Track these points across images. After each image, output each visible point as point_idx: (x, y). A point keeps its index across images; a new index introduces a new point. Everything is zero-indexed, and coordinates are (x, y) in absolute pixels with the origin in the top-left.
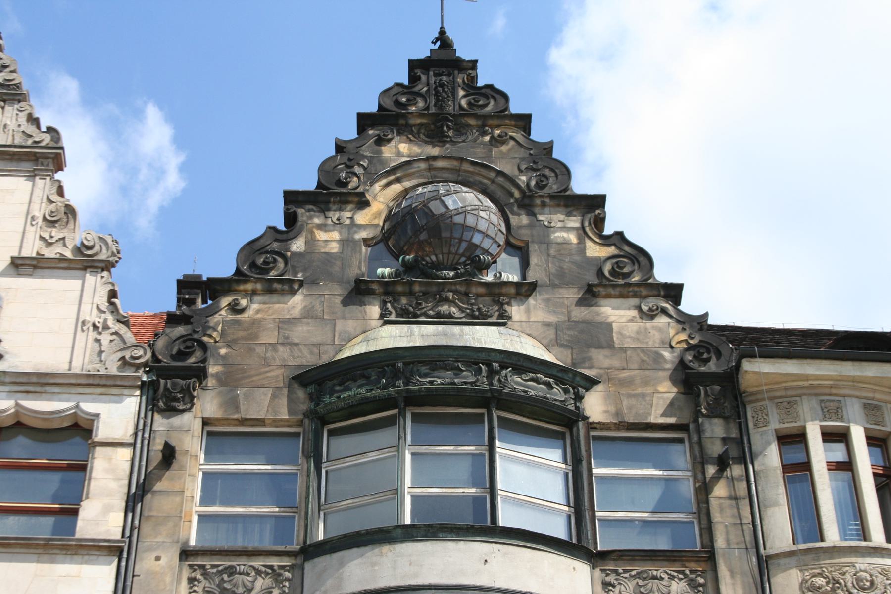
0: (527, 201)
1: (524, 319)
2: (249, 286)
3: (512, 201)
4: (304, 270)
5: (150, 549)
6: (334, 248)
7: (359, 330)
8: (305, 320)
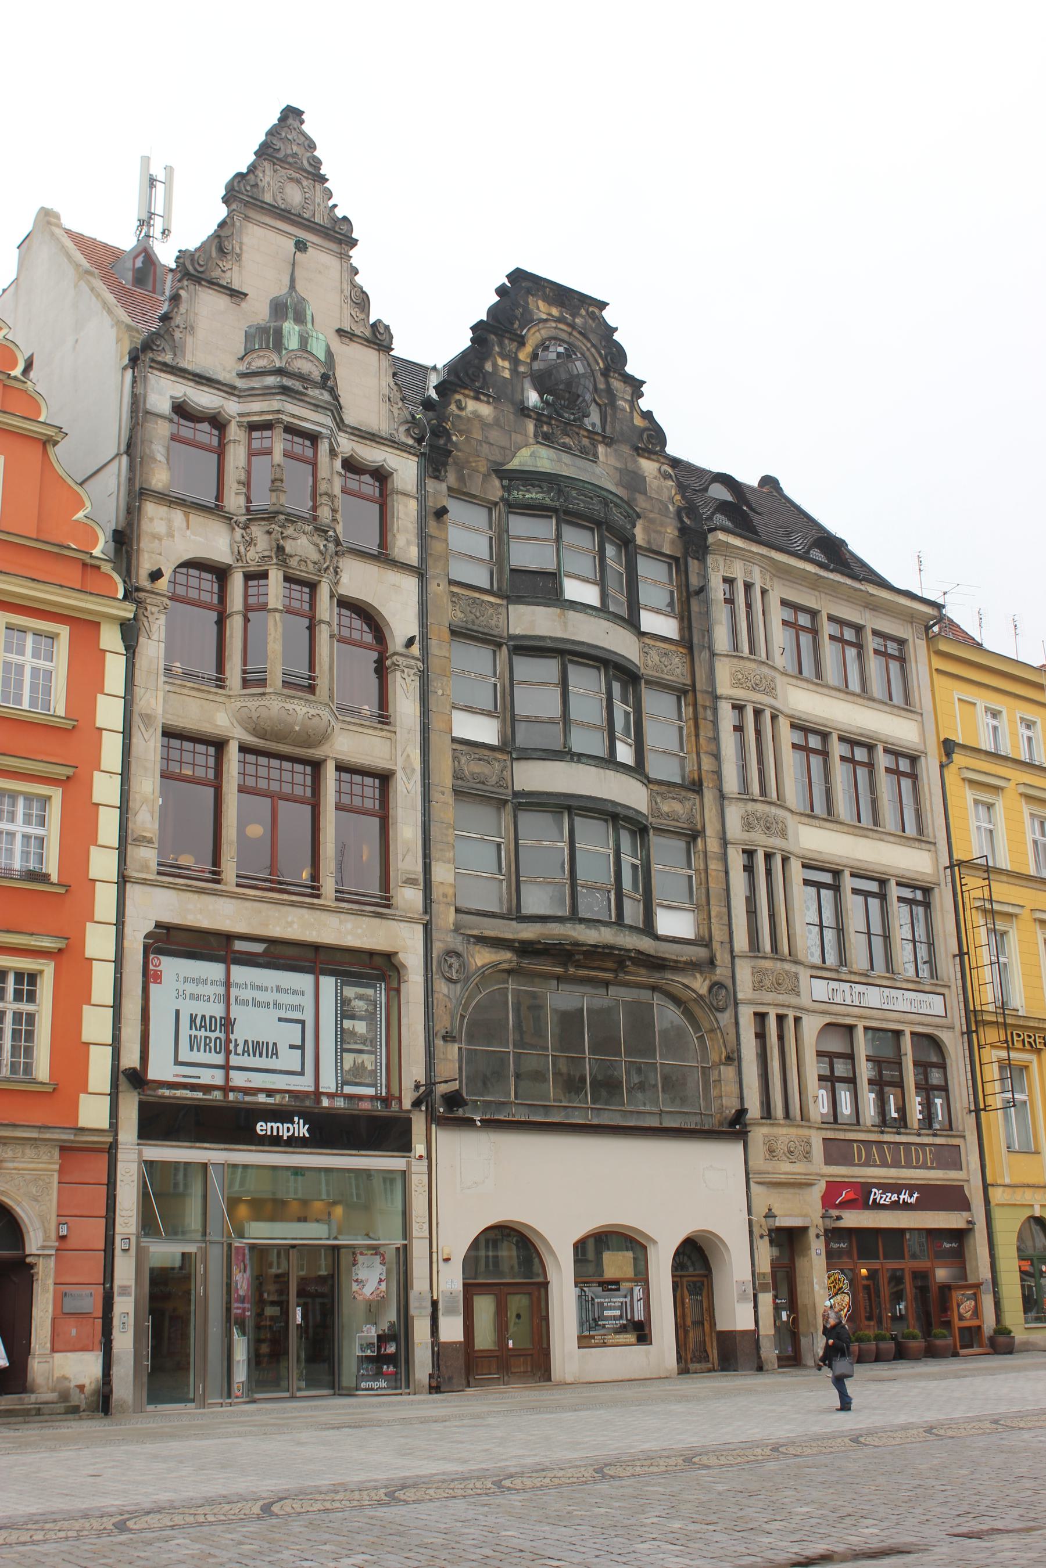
2: (467, 392)
5: (435, 578)
6: (507, 374)
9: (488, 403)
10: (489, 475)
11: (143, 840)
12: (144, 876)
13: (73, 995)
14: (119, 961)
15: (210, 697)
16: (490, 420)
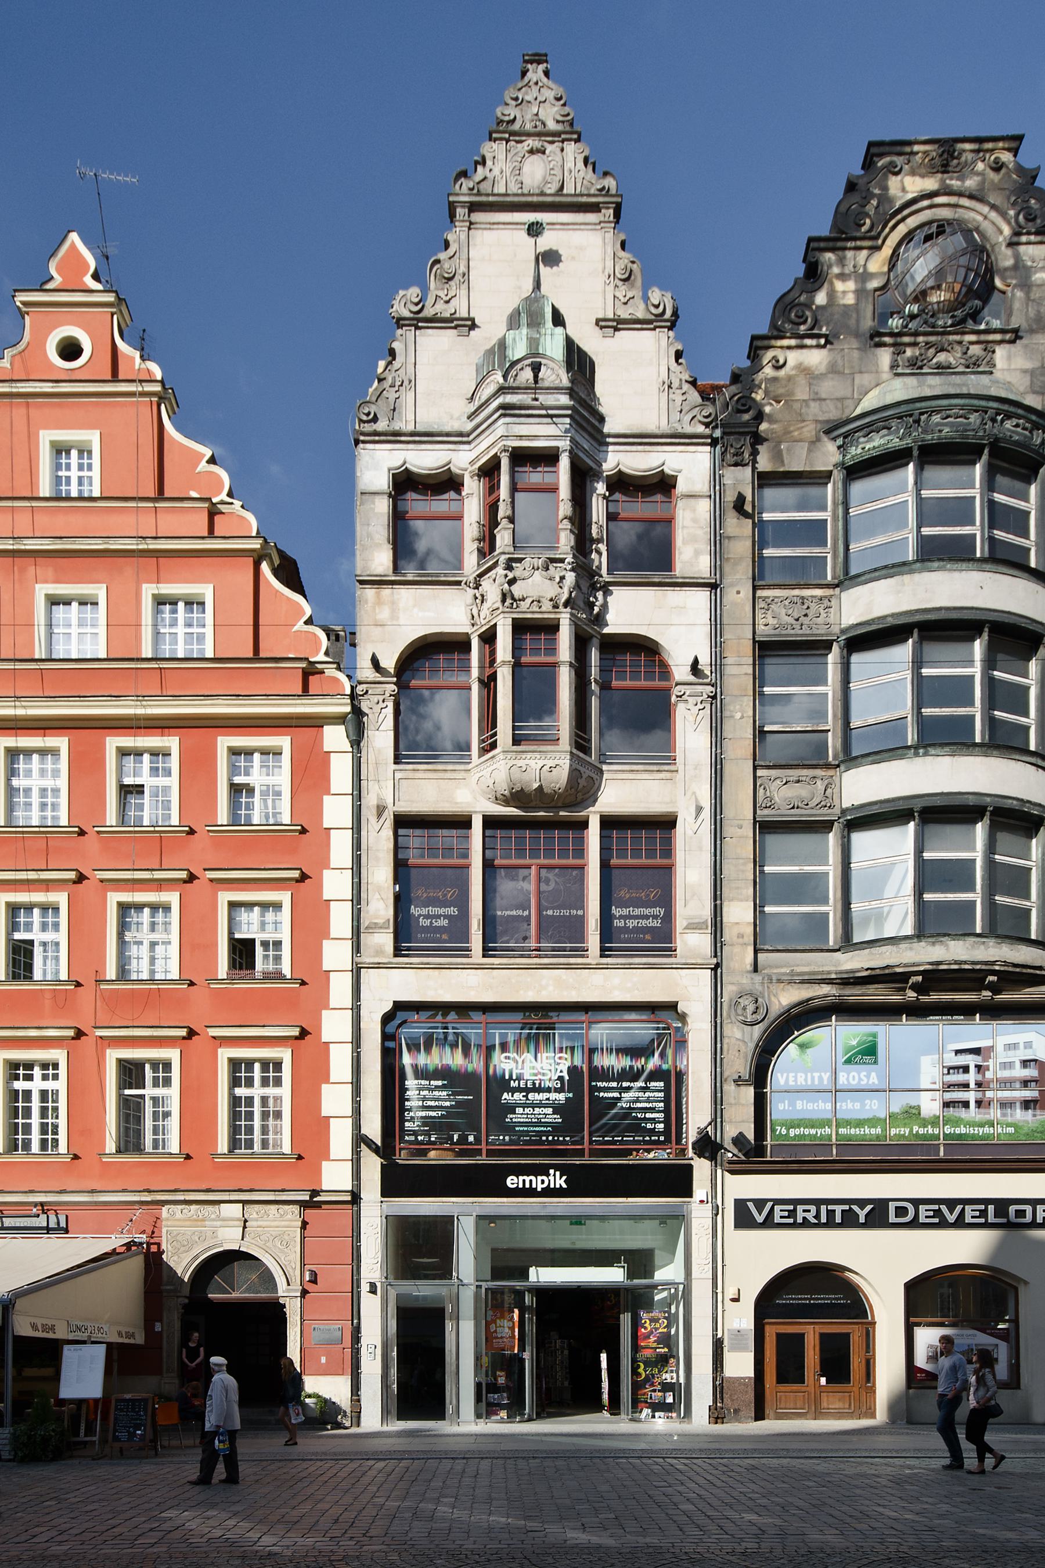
0: (1015, 239)
1: (1005, 367)
2: (785, 342)
3: (1001, 239)
4: (827, 324)
6: (850, 300)
7: (873, 383)
8: (830, 375)
9: (818, 346)
10: (818, 440)
11: (374, 927)
12: (376, 960)
13: (312, 1074)
14: (357, 1041)
15: (448, 775)
16: (823, 369)
